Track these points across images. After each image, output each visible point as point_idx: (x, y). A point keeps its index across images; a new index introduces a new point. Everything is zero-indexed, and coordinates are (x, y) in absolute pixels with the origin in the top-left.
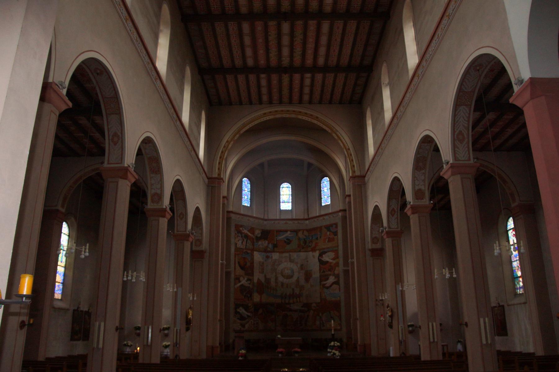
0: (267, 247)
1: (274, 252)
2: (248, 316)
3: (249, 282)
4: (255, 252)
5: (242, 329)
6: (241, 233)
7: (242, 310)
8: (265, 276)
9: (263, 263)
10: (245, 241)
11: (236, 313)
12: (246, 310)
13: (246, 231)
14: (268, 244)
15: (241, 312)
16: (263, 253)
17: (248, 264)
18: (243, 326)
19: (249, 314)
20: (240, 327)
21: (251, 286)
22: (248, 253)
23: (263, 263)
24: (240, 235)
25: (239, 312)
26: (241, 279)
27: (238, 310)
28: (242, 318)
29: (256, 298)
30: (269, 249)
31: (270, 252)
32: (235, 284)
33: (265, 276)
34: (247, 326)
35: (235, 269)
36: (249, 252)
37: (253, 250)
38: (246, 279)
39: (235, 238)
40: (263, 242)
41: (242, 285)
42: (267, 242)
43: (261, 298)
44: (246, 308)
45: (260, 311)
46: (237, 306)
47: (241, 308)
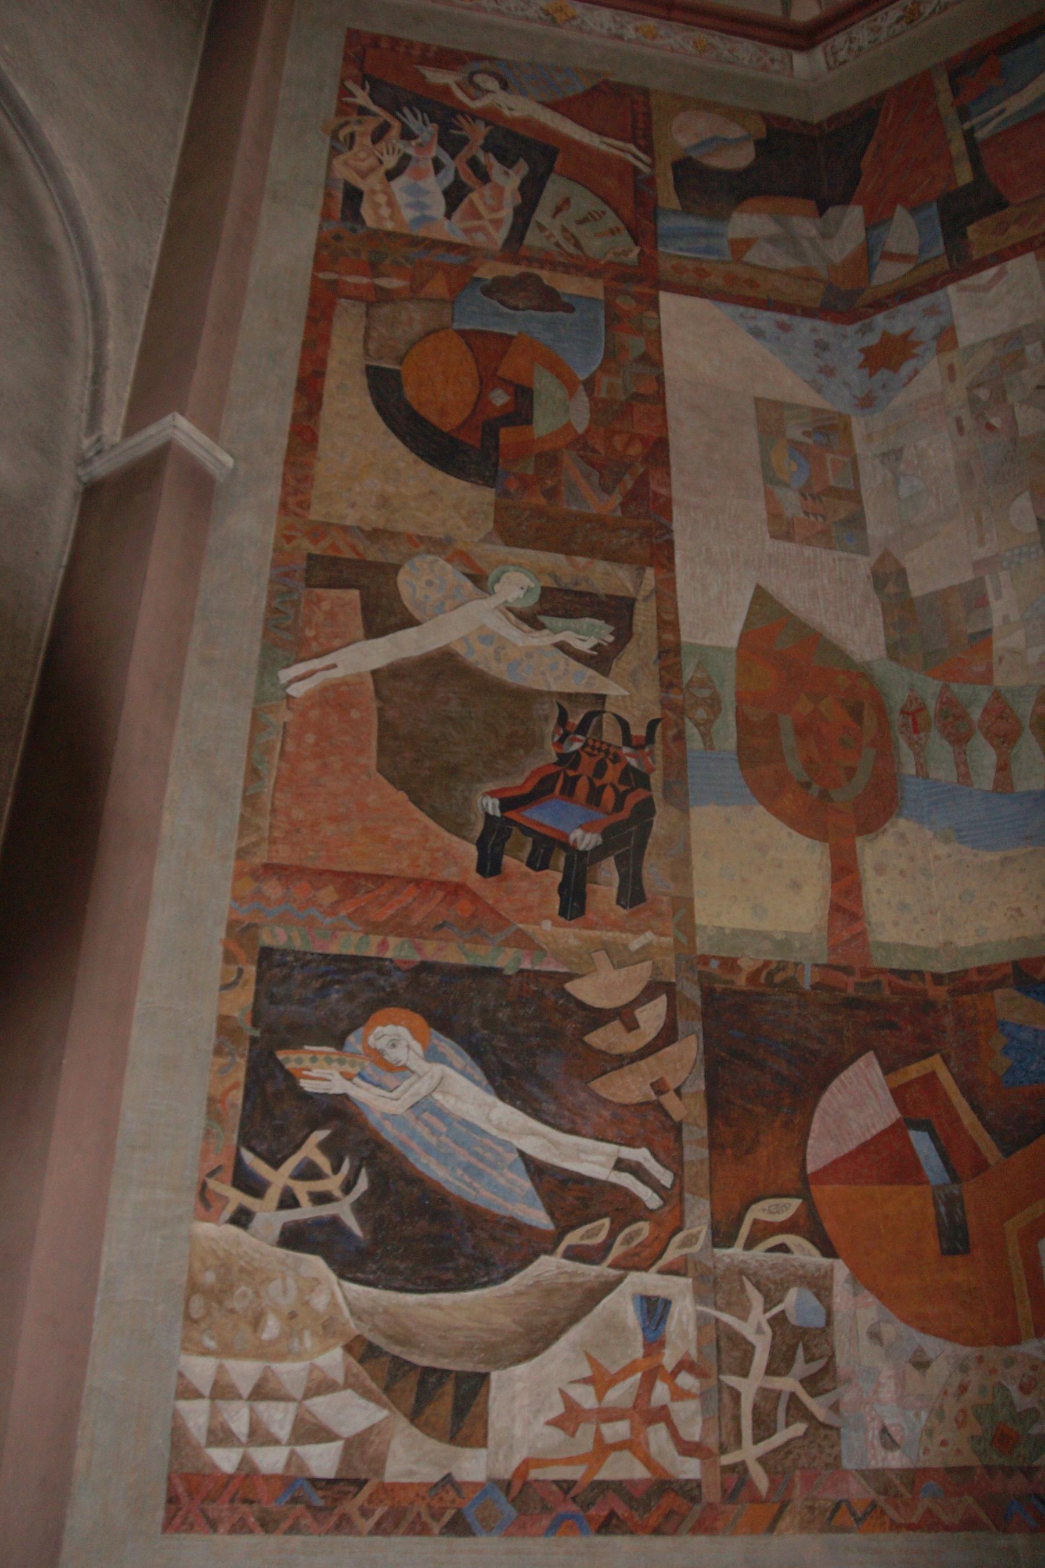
0: (868, 255)
1: (961, 265)
2: (570, 1196)
3: (588, 634)
4: (665, 298)
5: (412, 1457)
6: (447, 117)
7: (422, 1092)
8: (888, 578)
9: (830, 429)
10: (509, 182)
11: (272, 1113)
12: (509, 1081)
13: (518, 107)
14: (876, 220)
15: (380, 1104)
16: (804, 326)
17: (559, 413)
18: (449, 1399)
19: (591, 1159)
20: (354, 1413)
21: (629, 694)
22: (550, 300)
23: (830, 429)
24: (428, 132)
25: (338, 1112)
26: (417, 581)
27: (321, 1074)
28: (415, 1230)
29: (750, 884)
30: (888, 274)
31: (906, 294)
32: (286, 637)
33: (888, 578)
34: (525, 1413)
35: (304, 435)
36: (569, 286)
37: (642, 281)
38: (516, 587)
39: (340, 144)
40: (805, 226)
41: (444, 665)
42: (855, 214)
43: (845, 876)
44: (527, 1041)
45: (857, 1105)
46: (296, 1000)
47: (394, 1036)
